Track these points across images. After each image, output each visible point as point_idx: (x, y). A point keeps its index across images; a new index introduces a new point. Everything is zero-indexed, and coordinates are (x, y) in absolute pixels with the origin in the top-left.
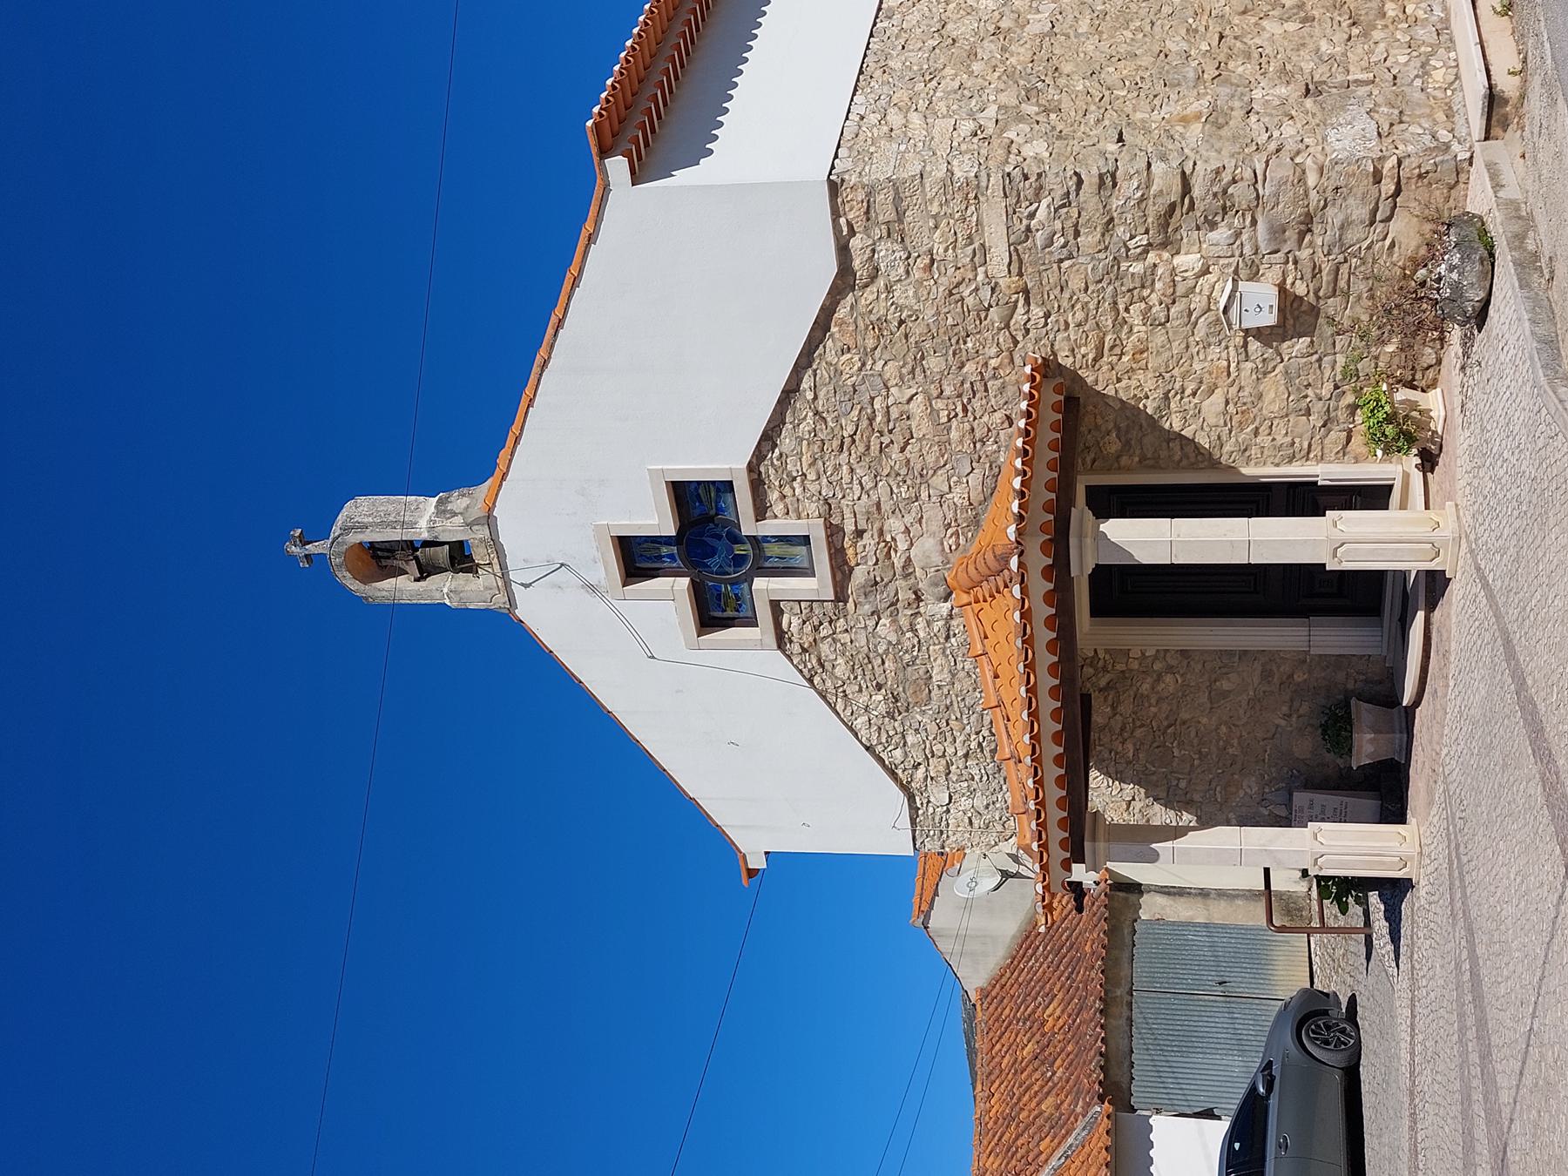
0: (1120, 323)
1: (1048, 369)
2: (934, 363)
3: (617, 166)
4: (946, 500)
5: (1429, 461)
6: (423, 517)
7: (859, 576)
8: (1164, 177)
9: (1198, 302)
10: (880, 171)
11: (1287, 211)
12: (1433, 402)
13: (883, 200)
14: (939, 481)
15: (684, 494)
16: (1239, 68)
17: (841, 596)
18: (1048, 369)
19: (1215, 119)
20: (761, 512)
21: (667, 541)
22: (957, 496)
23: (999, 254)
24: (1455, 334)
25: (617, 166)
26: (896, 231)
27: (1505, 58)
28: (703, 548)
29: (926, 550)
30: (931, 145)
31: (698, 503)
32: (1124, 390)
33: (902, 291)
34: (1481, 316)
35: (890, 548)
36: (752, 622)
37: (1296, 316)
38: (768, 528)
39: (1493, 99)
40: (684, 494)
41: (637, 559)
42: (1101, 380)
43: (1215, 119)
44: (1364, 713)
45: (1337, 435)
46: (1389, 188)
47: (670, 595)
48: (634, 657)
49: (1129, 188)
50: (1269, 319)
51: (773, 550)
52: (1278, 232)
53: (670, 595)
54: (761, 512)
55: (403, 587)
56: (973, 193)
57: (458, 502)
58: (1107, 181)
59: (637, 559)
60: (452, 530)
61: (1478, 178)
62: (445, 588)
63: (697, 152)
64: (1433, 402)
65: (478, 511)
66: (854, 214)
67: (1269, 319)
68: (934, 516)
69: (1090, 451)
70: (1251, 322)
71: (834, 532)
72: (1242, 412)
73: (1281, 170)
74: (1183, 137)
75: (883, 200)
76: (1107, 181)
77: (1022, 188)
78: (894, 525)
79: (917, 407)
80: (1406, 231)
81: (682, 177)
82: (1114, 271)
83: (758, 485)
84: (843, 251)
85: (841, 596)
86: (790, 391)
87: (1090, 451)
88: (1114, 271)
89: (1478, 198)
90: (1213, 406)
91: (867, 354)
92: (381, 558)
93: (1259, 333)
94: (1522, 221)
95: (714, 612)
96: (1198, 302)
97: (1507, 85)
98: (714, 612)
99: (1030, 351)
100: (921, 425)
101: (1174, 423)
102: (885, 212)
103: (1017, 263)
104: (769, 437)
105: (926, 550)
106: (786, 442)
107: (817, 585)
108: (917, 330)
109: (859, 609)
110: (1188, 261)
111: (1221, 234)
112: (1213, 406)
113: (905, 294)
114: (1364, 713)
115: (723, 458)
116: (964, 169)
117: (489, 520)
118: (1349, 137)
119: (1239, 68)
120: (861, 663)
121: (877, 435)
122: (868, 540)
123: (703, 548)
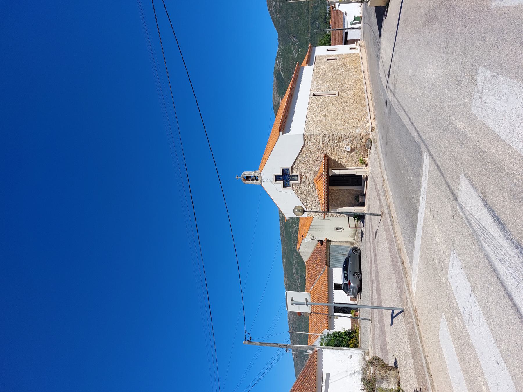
0: (334, 150)
1: (326, 156)
2: (313, 155)
3: (281, 133)
4: (313, 172)
5: (366, 166)
6: (253, 174)
7: (303, 180)
8: (339, 135)
9: (342, 148)
10: (309, 134)
11: (351, 139)
12: (367, 159)
13: (309, 136)
14: (313, 169)
15: (283, 170)
16: (346, 124)
17: (301, 183)
18: (326, 156)
19: (344, 129)
20: (292, 172)
21: (280, 176)
22: (315, 171)
23: (321, 143)
24: (369, 150)
25: (281, 133)
26: (310, 140)
27: (373, 123)
28: (285, 178)
29: (311, 177)
30: (314, 131)
31: (285, 171)
32: (334, 158)
33: (310, 147)
34: (371, 148)
35: (307, 177)
36: (290, 187)
37: (352, 150)
38: (293, 174)
39: (372, 127)
40: (283, 170)
41: (277, 178)
42: (331, 157)
43: (344, 129)
44: (360, 196)
45: (357, 163)
46: (362, 136)
47: (281, 183)
48: (275, 191)
49: (335, 136)
50: (350, 150)
51: (293, 177)
52: (351, 141)
53: (281, 183)
54: (292, 172)
55: (249, 182)
56: (319, 136)
57: (257, 172)
58: (333, 135)
59: (277, 178)
60: (256, 175)
61: (371, 135)
62: (254, 182)
63: (289, 132)
64: (367, 159)
65: (259, 172)
66: (306, 138)
67: (350, 150)
68: (312, 173)
69: (330, 163)
70: (348, 150)
71: (300, 175)
72: (347, 161)
73: (351, 134)
74: (340, 131)
75: (309, 136)
76: (333, 135)
77: (324, 136)
78: (307, 174)
79: (311, 160)
80: (363, 141)
81: (287, 134)
82: (333, 145)
83: (292, 169)
84: (304, 142)
85: (301, 183)
86: (297, 158)
87: (330, 163)
88: (333, 145)
89: (371, 137)
90: (343, 160)
91: (306, 154)
92: (247, 178)
93: (348, 152)
94: (374, 138)
95: (285, 186)
96: (342, 148)
97: (373, 126)
98: (285, 186)
99: (324, 153)
100: (311, 162)
101: (339, 162)
102: (309, 138)
103: (323, 144)
104: (294, 164)
105: (311, 177)
106: (296, 164)
107: (298, 182)
108: (312, 151)
109: (302, 185)
110: (341, 144)
111: (345, 141)
112: (343, 160)
113: (311, 147)
114: (360, 196)
115: (288, 166)
116: (318, 134)
117: (261, 173)
118: (358, 131)
119: (346, 124)
120: (302, 192)
121: (306, 163)
122: (304, 176)
123: (285, 178)
